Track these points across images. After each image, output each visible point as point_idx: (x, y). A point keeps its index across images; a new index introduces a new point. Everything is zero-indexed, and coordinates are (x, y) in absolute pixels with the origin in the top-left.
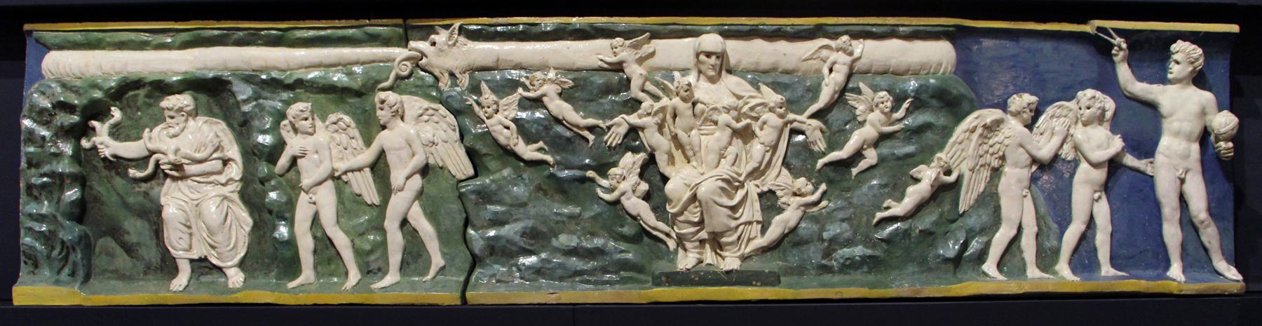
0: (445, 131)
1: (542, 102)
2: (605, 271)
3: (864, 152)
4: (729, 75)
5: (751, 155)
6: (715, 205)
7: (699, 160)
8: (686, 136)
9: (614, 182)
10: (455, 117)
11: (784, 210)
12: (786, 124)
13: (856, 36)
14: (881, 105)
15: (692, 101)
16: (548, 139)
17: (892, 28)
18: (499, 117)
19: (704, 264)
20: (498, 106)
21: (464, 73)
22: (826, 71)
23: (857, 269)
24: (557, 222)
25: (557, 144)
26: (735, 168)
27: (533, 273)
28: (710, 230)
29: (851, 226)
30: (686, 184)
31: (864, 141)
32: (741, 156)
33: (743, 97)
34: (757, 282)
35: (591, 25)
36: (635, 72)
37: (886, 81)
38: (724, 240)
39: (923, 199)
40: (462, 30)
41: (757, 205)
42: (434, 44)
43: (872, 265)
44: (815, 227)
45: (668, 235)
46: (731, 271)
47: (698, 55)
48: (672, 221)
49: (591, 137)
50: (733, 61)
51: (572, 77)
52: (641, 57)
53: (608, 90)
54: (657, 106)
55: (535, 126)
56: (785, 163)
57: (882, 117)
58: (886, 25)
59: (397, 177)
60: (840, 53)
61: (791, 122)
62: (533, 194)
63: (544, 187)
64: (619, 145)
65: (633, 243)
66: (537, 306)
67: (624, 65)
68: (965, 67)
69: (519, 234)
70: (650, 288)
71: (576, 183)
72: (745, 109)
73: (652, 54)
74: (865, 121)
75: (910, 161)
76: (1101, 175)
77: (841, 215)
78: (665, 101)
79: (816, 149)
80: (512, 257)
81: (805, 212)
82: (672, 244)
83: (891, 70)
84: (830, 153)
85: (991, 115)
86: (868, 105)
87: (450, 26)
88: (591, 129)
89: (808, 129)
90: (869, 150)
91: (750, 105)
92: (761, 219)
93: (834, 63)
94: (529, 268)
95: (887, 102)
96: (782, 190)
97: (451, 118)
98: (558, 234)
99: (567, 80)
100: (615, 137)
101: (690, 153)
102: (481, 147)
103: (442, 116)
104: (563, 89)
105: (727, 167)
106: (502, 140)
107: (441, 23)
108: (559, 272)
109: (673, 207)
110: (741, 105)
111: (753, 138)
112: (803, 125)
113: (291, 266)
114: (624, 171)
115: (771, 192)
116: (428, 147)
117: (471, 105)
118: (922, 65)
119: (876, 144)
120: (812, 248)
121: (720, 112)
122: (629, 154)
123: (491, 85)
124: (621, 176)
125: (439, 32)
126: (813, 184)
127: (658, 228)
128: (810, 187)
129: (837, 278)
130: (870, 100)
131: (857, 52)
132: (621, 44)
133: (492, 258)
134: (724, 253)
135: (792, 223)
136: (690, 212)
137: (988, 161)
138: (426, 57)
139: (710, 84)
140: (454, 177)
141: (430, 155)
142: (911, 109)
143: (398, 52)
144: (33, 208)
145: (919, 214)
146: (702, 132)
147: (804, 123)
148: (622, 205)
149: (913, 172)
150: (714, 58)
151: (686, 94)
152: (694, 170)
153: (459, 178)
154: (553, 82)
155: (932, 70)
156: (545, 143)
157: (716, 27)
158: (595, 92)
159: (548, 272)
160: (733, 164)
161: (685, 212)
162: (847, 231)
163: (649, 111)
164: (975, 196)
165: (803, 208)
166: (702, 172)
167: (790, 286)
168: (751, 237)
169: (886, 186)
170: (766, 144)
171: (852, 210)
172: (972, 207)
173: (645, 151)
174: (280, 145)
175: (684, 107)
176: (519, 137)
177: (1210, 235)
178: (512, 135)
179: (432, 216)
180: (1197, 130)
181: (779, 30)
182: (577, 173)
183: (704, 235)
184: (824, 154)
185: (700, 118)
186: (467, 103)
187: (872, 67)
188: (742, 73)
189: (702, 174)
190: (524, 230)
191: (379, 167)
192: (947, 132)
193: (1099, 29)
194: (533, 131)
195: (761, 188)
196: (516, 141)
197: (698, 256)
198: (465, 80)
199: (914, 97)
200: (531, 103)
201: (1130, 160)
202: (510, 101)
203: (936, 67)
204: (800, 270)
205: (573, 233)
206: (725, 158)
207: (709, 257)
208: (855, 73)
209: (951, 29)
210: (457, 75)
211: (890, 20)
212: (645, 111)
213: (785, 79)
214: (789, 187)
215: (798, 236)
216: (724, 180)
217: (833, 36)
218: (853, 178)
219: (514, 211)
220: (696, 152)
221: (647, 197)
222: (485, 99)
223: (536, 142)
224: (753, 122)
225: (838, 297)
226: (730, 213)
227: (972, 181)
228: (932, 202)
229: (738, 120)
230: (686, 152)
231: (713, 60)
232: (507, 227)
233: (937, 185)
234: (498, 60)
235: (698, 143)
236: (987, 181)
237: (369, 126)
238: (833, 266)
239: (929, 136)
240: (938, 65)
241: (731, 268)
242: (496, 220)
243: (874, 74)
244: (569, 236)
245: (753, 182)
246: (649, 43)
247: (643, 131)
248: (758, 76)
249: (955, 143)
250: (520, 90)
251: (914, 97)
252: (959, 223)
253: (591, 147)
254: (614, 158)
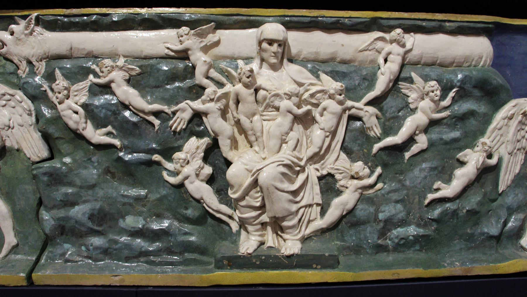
0: (21, 116)
1: (111, 88)
2: (170, 252)
3: (416, 138)
4: (290, 64)
5: (311, 139)
6: (277, 191)
7: (261, 145)
8: (248, 121)
9: (178, 166)
10: (32, 102)
11: (342, 192)
12: (344, 111)
13: (408, 29)
14: (431, 94)
15: (254, 87)
16: (116, 124)
17: (439, 23)
18: (69, 102)
19: (265, 247)
20: (69, 92)
21: (41, 61)
22: (381, 61)
23: (409, 248)
24: (124, 204)
26: (296, 153)
27: (101, 253)
28: (271, 215)
29: (405, 207)
30: (247, 170)
31: (417, 127)
32: (302, 141)
33: (305, 84)
34: (317, 265)
35: (159, 15)
37: (434, 72)
38: (285, 224)
39: (470, 181)
40: (38, 21)
41: (317, 189)
42: (12, 34)
43: (423, 244)
44: (372, 209)
45: (231, 217)
46: (292, 255)
47: (260, 43)
49: (157, 122)
50: (294, 51)
51: (139, 64)
52: (206, 45)
53: (173, 77)
54: (220, 92)
55: (104, 111)
56: (344, 148)
57: (432, 105)
58: (434, 20)
60: (394, 44)
61: (350, 109)
62: (102, 177)
63: (112, 170)
64: (185, 129)
65: (198, 225)
66: (101, 288)
67: (190, 52)
69: (87, 216)
70: (211, 271)
71: (143, 166)
72: (306, 96)
73: (217, 43)
74: (416, 108)
75: (456, 145)
77: (395, 196)
78: (228, 87)
79: (372, 134)
80: (81, 237)
81: (361, 194)
82: (234, 226)
83: (438, 62)
84: (384, 138)
86: (421, 93)
87: (28, 16)
88: (157, 114)
89: (366, 115)
90: (420, 135)
91: (310, 92)
92: (320, 202)
93: (389, 53)
94: (96, 248)
95: (437, 90)
96: (341, 173)
97: (28, 104)
98: (125, 216)
99: (135, 67)
101: (253, 138)
103: (18, 101)
104: (131, 76)
105: (288, 152)
106: (72, 124)
107: (20, 14)
108: (126, 253)
109: (234, 193)
110: (301, 92)
111: (313, 124)
112: (360, 111)
114: (188, 155)
115: (330, 175)
116: (4, 131)
117: (46, 91)
118: (465, 58)
119: (426, 130)
120: (369, 229)
121: (281, 98)
122: (193, 139)
123: (64, 72)
124: (185, 160)
125: (20, 22)
126: (369, 168)
127: (221, 211)
128: (367, 171)
129: (390, 258)
130: (422, 88)
131: (408, 46)
132: (186, 32)
133: (63, 237)
134: (285, 236)
135: (350, 206)
136: (251, 197)
137: (524, 145)
138: (6, 45)
139: (272, 72)
140: (29, 159)
141: (7, 138)
142: (456, 98)
145: (465, 195)
146: (264, 118)
147: (362, 109)
148: (186, 189)
149: (460, 155)
150: (276, 45)
151: (248, 80)
152: (257, 154)
153: (33, 160)
154: (121, 68)
155: (474, 63)
156: (114, 127)
157: (278, 18)
158: (161, 79)
159: (115, 252)
160: (294, 149)
161: (247, 198)
162: (401, 212)
163: (212, 97)
164: (511, 177)
165: (360, 191)
166: (263, 157)
167: (349, 268)
168: (311, 219)
169: (436, 168)
170: (326, 130)
171: (405, 192)
172: (509, 187)
173: (209, 136)
175: (246, 93)
176: (89, 121)
178: (81, 119)
181: (337, 22)
182: (142, 156)
183: (265, 218)
184: (379, 139)
185: (262, 104)
186: (42, 89)
187: (421, 58)
188: (303, 62)
189: (264, 159)
190: (92, 212)
192: (487, 120)
194: (102, 115)
195: (320, 171)
196: (84, 125)
197: (260, 239)
198: (42, 67)
199: (459, 87)
200: (101, 89)
202: (81, 87)
203: (477, 60)
204: (357, 250)
205: (140, 214)
206: (286, 143)
207: (271, 239)
208: (407, 64)
209: (490, 26)
210: (34, 63)
211: (437, 16)
212: (208, 96)
213: (343, 68)
214: (348, 171)
215: (355, 216)
216: (285, 166)
217: (387, 29)
218: (406, 161)
219: (83, 193)
220: (259, 137)
221: (210, 181)
222: (56, 85)
223: (105, 126)
224: (313, 108)
225: (395, 277)
226: (290, 197)
227: (510, 164)
228: (476, 183)
229: (299, 107)
230: (249, 137)
231: (275, 48)
232: (77, 208)
233: (482, 167)
234: (71, 49)
235: (260, 128)
236: (522, 163)
238: (388, 245)
239: (472, 122)
240: (479, 58)
241: (292, 253)
242: (67, 201)
243: (423, 65)
244: (136, 217)
245: (313, 166)
246: (214, 32)
247: (206, 117)
249: (495, 128)
250: (91, 77)
251: (459, 87)
252: (499, 201)
253: (157, 132)
254: (180, 142)
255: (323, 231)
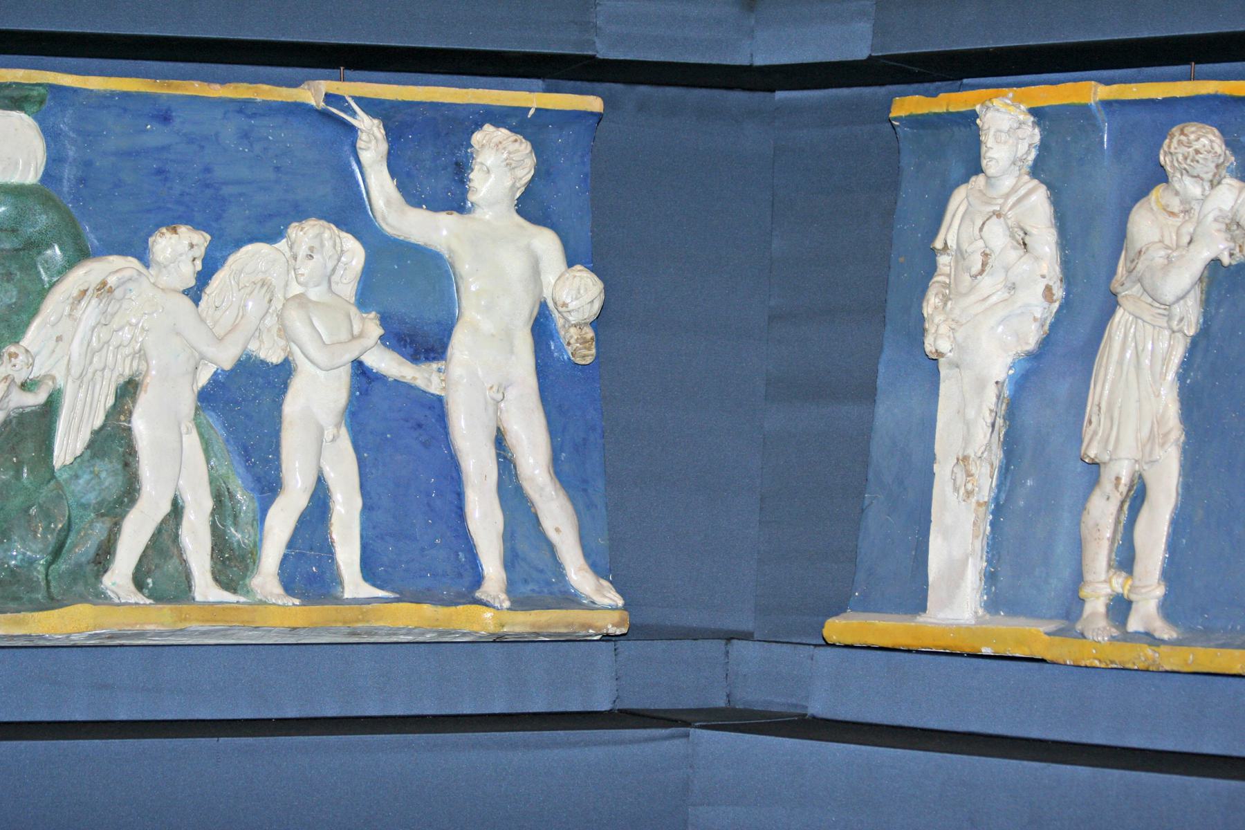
164: (85, 437)
193: (329, 98)
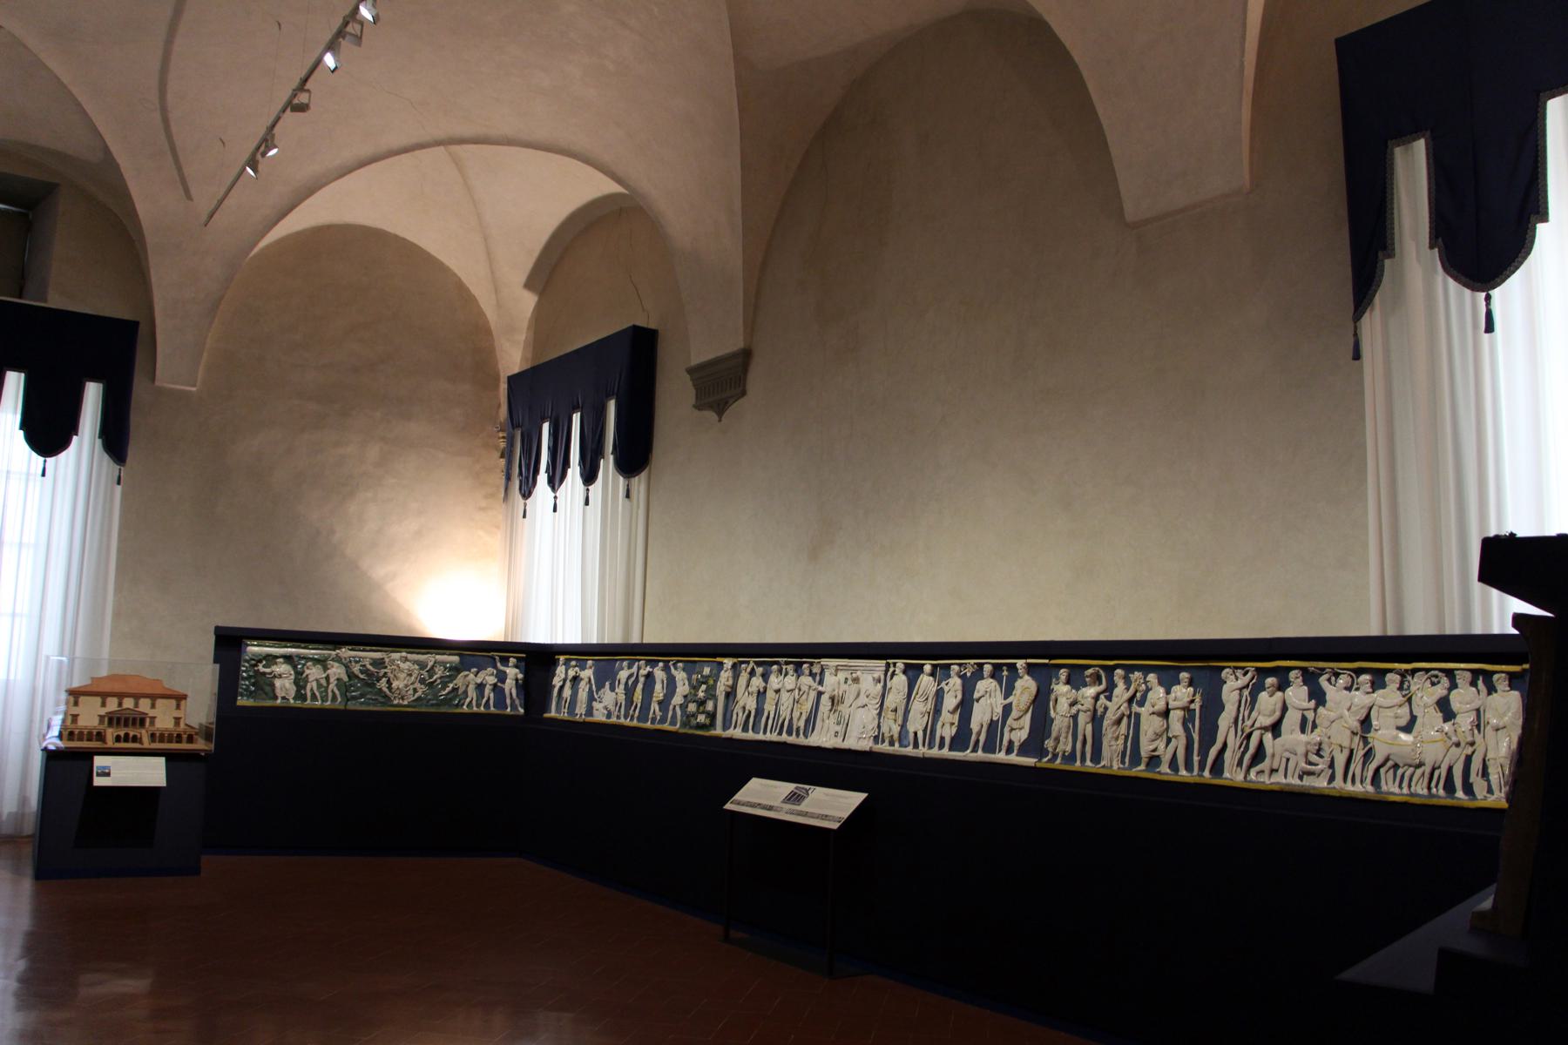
25: (368, 675)
36: (387, 660)
48: (393, 693)
59: (332, 680)
68: (461, 662)
76: (491, 687)
85: (467, 673)
100: (381, 674)
102: (351, 675)
113: (305, 699)
143: (333, 653)
144: (243, 683)
174: (303, 672)
177: (517, 702)
179: (339, 690)
180: (514, 678)
191: (327, 678)
198: (348, 660)
201: (499, 684)
204: (421, 705)
207: (401, 701)
237: (325, 668)
248: (415, 662)
255: (413, 701)
